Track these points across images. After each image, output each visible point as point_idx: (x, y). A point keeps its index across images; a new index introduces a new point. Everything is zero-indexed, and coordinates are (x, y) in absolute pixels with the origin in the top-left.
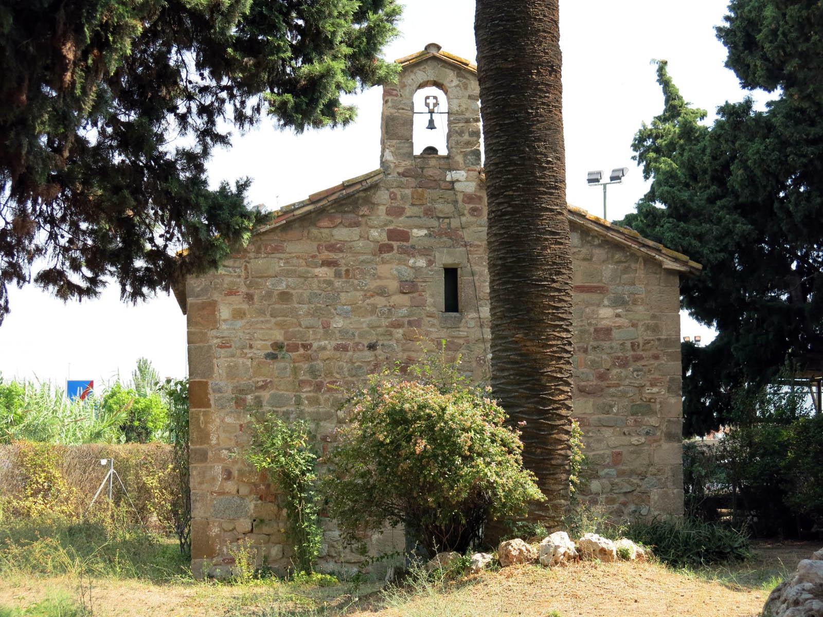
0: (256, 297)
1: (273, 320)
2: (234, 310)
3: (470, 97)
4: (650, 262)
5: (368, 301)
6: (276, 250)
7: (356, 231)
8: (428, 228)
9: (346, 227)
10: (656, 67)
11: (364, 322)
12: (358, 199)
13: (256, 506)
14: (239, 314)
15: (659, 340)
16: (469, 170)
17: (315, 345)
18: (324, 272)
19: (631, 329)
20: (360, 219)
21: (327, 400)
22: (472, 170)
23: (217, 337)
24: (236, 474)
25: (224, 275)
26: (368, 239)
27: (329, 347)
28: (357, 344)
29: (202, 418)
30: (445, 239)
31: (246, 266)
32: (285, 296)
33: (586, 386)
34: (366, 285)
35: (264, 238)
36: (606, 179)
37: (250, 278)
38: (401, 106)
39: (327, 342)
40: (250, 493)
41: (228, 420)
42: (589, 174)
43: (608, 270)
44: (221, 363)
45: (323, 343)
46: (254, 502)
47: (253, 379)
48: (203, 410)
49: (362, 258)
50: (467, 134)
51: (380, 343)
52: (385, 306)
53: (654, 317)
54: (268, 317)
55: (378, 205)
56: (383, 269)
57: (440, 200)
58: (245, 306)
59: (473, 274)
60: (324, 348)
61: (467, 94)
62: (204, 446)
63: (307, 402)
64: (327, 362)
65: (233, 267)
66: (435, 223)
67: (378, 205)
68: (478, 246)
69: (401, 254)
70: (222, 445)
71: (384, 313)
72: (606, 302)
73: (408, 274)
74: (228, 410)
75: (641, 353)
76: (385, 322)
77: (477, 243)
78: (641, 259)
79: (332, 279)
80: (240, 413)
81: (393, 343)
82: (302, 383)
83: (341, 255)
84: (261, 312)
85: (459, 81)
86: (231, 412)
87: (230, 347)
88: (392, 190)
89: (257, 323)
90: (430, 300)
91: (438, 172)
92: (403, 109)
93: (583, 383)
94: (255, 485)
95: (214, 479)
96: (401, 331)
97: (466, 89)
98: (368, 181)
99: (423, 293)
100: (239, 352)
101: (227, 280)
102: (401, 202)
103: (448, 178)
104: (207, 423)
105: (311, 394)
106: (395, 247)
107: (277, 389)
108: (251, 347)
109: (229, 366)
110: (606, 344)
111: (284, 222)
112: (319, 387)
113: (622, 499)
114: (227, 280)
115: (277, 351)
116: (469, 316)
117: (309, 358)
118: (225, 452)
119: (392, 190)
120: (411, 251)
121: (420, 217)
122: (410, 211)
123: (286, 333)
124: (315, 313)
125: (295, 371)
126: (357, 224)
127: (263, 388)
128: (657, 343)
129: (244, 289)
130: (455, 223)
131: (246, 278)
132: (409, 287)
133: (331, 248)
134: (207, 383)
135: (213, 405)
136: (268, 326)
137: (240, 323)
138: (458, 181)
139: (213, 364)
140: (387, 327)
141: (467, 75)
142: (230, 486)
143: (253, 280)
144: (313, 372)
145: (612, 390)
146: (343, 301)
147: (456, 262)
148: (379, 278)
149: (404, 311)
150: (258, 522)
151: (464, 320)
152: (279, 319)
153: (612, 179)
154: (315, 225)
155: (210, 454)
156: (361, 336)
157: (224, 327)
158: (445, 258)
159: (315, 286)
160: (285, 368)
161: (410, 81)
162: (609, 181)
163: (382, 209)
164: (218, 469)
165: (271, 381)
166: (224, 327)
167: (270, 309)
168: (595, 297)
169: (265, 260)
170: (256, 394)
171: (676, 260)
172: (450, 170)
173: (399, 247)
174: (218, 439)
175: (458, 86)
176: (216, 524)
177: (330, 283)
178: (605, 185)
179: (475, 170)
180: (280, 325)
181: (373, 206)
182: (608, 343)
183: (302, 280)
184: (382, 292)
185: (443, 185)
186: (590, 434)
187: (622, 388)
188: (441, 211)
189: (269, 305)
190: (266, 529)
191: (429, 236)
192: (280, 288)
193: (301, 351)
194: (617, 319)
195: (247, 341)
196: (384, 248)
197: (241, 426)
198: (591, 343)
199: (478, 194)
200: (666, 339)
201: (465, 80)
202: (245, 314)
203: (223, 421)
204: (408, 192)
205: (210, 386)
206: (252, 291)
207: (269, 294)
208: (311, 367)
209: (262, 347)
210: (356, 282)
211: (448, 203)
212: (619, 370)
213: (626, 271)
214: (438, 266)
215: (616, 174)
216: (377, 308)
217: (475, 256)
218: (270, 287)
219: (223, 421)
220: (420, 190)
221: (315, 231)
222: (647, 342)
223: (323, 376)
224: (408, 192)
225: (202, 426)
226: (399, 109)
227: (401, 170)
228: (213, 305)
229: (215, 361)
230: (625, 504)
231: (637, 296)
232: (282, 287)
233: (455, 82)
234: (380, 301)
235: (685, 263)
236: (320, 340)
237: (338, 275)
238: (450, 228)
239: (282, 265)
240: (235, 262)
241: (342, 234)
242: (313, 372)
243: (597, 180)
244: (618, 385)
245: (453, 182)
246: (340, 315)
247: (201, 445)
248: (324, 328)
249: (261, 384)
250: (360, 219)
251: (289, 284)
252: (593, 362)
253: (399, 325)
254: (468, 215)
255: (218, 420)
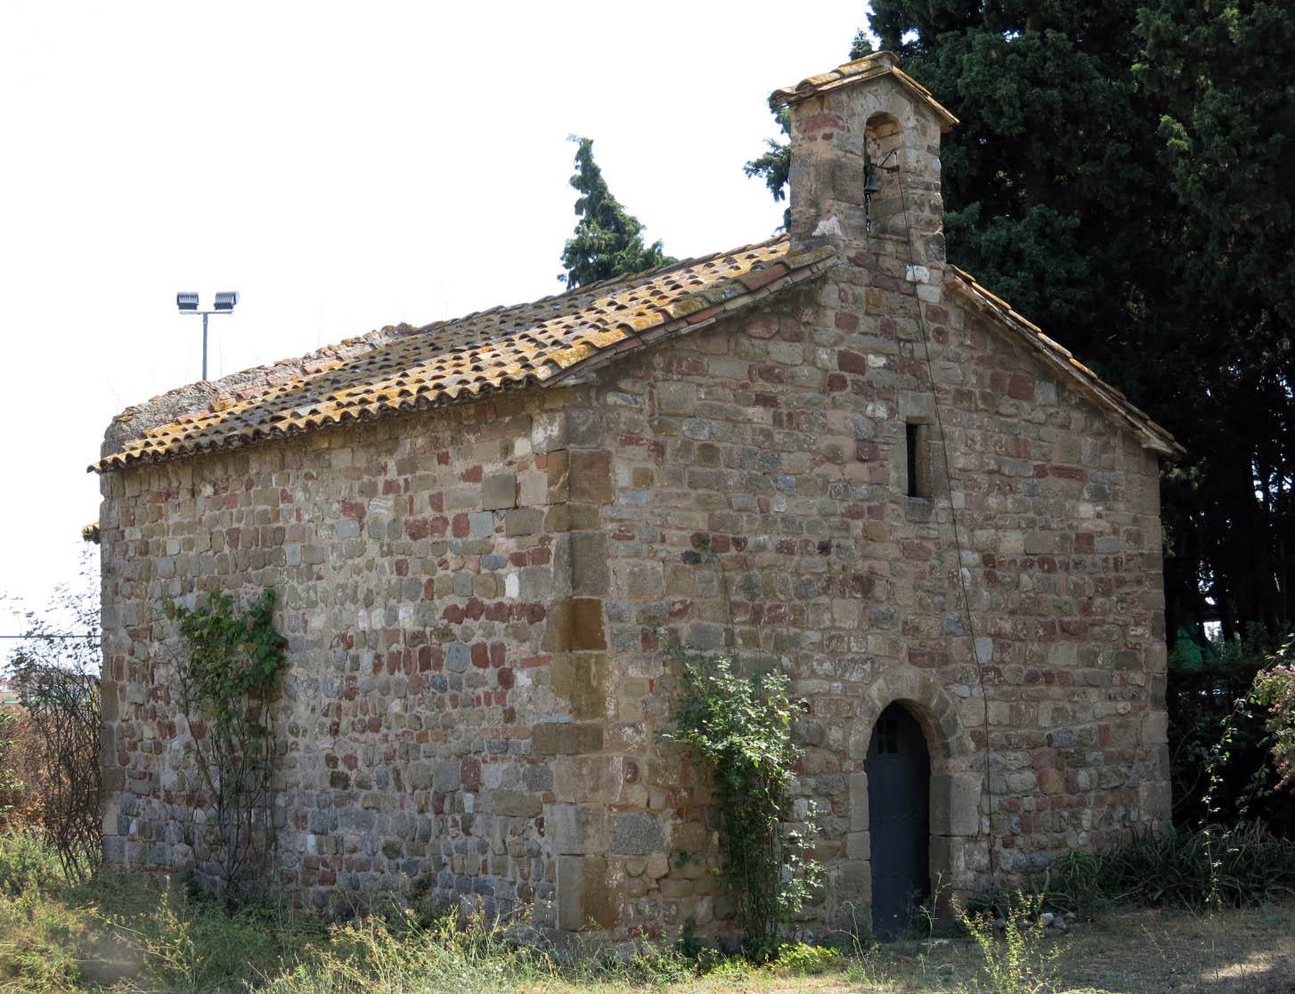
0: (668, 450)
1: (693, 494)
2: (636, 471)
3: (929, 148)
4: (1131, 438)
5: (817, 470)
6: (696, 368)
7: (798, 348)
8: (887, 356)
9: (785, 340)
10: (576, 147)
11: (814, 504)
12: (799, 292)
13: (675, 829)
14: (643, 479)
15: (1142, 554)
16: (931, 267)
17: (751, 542)
18: (757, 414)
19: (1113, 537)
20: (803, 329)
21: (767, 638)
22: (936, 268)
23: (612, 520)
24: (645, 771)
25: (621, 406)
26: (814, 364)
27: (770, 546)
28: (807, 542)
29: (594, 668)
30: (908, 376)
31: (651, 393)
32: (709, 453)
33: (1069, 623)
34: (814, 443)
35: (679, 345)
36: (206, 303)
37: (657, 415)
38: (849, 147)
39: (767, 537)
40: (666, 806)
41: (633, 672)
42: (219, 296)
43: (1087, 444)
44: (620, 565)
45: (761, 538)
46: (672, 821)
47: (667, 599)
48: (595, 652)
49: (808, 395)
50: (927, 208)
51: (834, 542)
52: (840, 480)
53: (1135, 520)
54: (686, 489)
55: (825, 307)
56: (836, 418)
57: (901, 311)
58: (651, 466)
59: (942, 436)
60: (762, 548)
61: (925, 144)
62: (597, 721)
63: (740, 641)
64: (766, 572)
65: (633, 394)
66: (893, 347)
67: (825, 307)
68: (948, 392)
69: (857, 394)
70: (623, 718)
71: (839, 493)
72: (1086, 495)
73: (867, 430)
74: (631, 653)
75: (1124, 574)
76: (841, 508)
77: (945, 386)
78: (1119, 432)
79: (770, 428)
80: (650, 659)
81: (851, 543)
82: (734, 608)
83: (781, 388)
84: (676, 478)
85: (917, 120)
86: (636, 658)
87: (632, 538)
88: (842, 285)
89: (671, 496)
90: (893, 475)
91: (897, 263)
92: (851, 152)
93: (1066, 619)
94: (674, 790)
95: (612, 780)
96: (860, 523)
97: (924, 134)
98: (820, 265)
99: (885, 463)
100: (645, 547)
101: (625, 415)
102: (854, 307)
103: (909, 277)
104: (600, 677)
105: (746, 628)
106: (849, 383)
107: (700, 617)
108: (663, 540)
109: (632, 574)
110: (1089, 559)
111: (713, 320)
112: (757, 614)
113: (1110, 798)
114: (625, 415)
115: (701, 548)
116: (940, 505)
117: (744, 564)
118: (629, 731)
119: (842, 285)
120: (867, 391)
121: (876, 335)
122: (866, 324)
123: (711, 517)
124: (750, 485)
125: (725, 585)
126: (796, 338)
127: (680, 614)
128: (1140, 559)
129: (648, 435)
130: (919, 350)
131: (651, 416)
132: (868, 451)
133: (768, 374)
134: (599, 602)
135: (609, 645)
136: (687, 503)
137: (646, 496)
138: (920, 282)
139: (608, 569)
140: (843, 515)
141: (926, 113)
142: (638, 795)
143: (663, 420)
144: (749, 587)
145: (1097, 629)
146: (786, 467)
147: (922, 415)
148: (831, 431)
149: (863, 490)
150: (681, 857)
151: (933, 511)
152: (700, 491)
153: (218, 306)
154: (744, 331)
155: (606, 736)
156: (813, 527)
157: (622, 501)
158: (910, 408)
159: (748, 437)
160: (712, 580)
161: (858, 109)
162: (212, 309)
163: (831, 314)
164: (618, 761)
165: (691, 603)
166: (622, 501)
167: (687, 474)
168: (1075, 484)
169: (680, 385)
170: (671, 625)
171: (1162, 437)
172: (912, 263)
173: (854, 382)
174: (617, 705)
175: (914, 128)
176: (618, 865)
177: (768, 435)
178: (206, 315)
179: (938, 269)
180: (703, 503)
181: (818, 308)
182: (1090, 556)
183: (730, 425)
184: (834, 456)
185: (904, 286)
186: (1076, 698)
187: (1106, 627)
188: (903, 330)
189: (686, 466)
190: (691, 870)
191: (887, 367)
192: (702, 438)
193: (733, 551)
194: (1099, 521)
195: (657, 529)
196: (835, 383)
197: (651, 682)
198: (1073, 556)
199: (944, 308)
200: (1149, 555)
201: (923, 121)
202: (652, 480)
203: (624, 674)
204: (861, 291)
205: (604, 609)
206: (661, 439)
207: (686, 447)
208: (748, 579)
209: (678, 543)
210: (801, 436)
211: (910, 317)
212: (1102, 600)
213: (1105, 448)
214: (900, 421)
215: (224, 300)
216: (829, 482)
217: (944, 407)
218: (687, 433)
219: (624, 674)
220: (876, 290)
221: (744, 341)
222: (1130, 558)
223: (762, 596)
224: (861, 291)
225: (594, 683)
226: (846, 151)
227: (852, 254)
228: (603, 461)
229: (609, 562)
230: (1113, 806)
231: (1117, 487)
232: (703, 436)
233: (912, 123)
234: (832, 470)
235: (1170, 444)
236: (756, 534)
237: (777, 420)
238: (912, 358)
239: (703, 396)
240: (634, 383)
241: (782, 351)
242: (749, 587)
243: (194, 306)
244: (1103, 622)
245: (915, 284)
246: (782, 491)
247: (593, 717)
248: (762, 512)
249: (678, 606)
250: (803, 329)
251: (714, 431)
252: (1076, 585)
253: (855, 514)
254: (932, 340)
255: (616, 672)
